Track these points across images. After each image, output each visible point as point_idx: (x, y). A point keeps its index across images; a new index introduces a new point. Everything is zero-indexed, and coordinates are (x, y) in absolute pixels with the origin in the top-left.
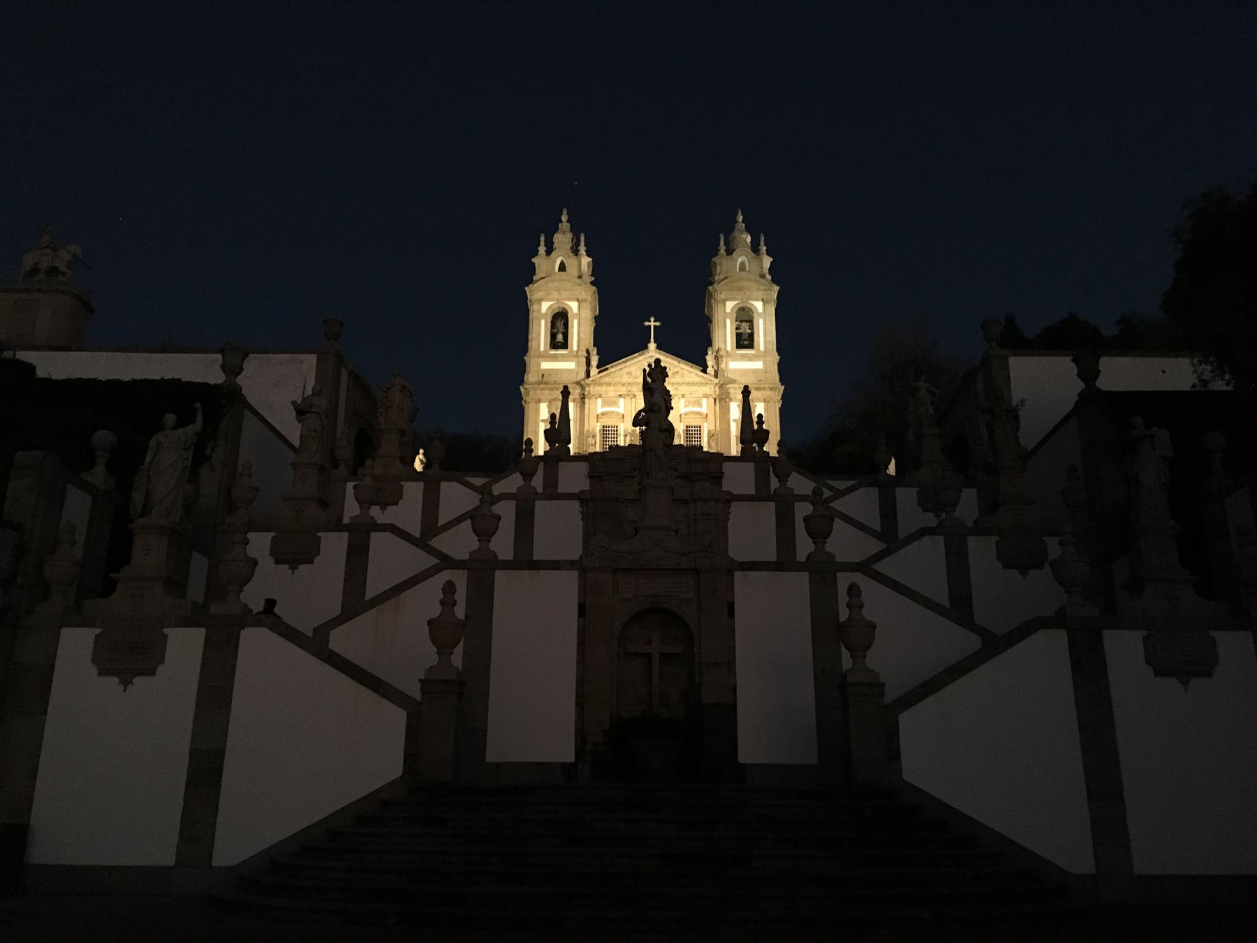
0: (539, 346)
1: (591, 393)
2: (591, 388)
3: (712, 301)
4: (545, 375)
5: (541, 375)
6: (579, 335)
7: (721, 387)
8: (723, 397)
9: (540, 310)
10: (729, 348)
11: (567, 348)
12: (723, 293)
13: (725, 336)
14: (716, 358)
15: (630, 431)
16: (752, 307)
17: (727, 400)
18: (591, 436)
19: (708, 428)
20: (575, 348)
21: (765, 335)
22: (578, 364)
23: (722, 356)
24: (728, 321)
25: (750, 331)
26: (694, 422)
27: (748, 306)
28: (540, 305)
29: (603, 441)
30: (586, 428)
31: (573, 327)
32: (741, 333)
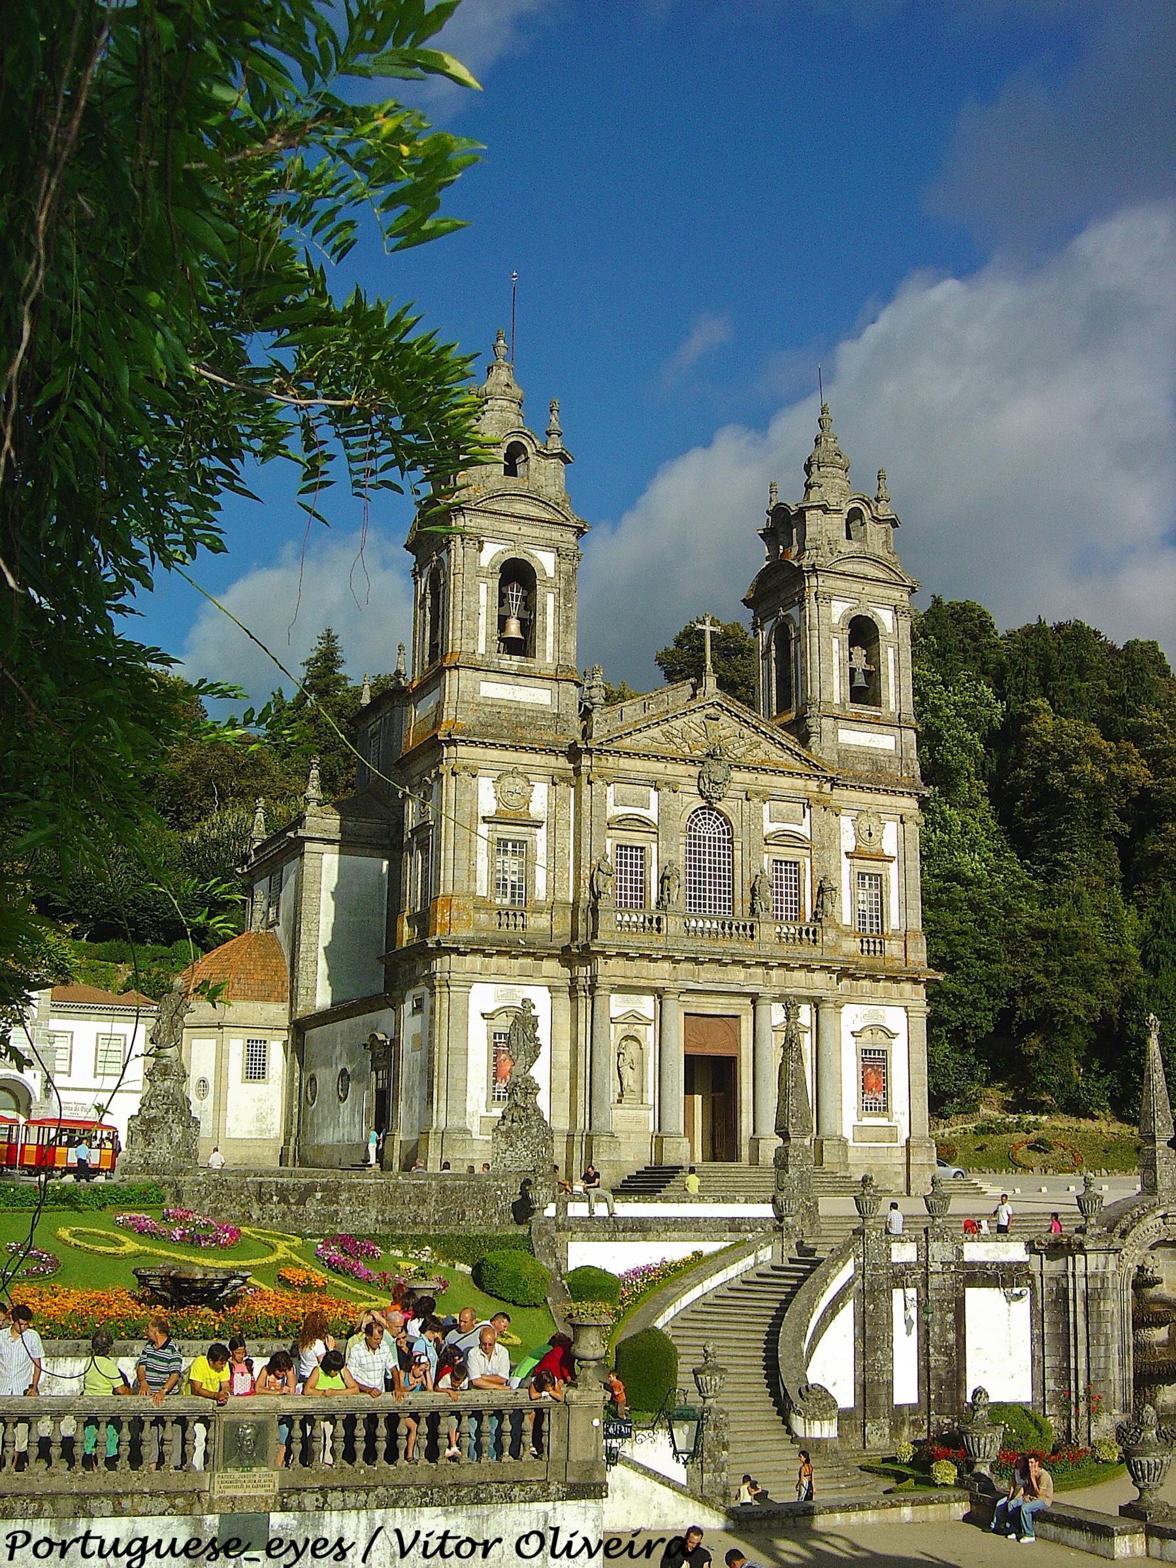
9: (476, 560)
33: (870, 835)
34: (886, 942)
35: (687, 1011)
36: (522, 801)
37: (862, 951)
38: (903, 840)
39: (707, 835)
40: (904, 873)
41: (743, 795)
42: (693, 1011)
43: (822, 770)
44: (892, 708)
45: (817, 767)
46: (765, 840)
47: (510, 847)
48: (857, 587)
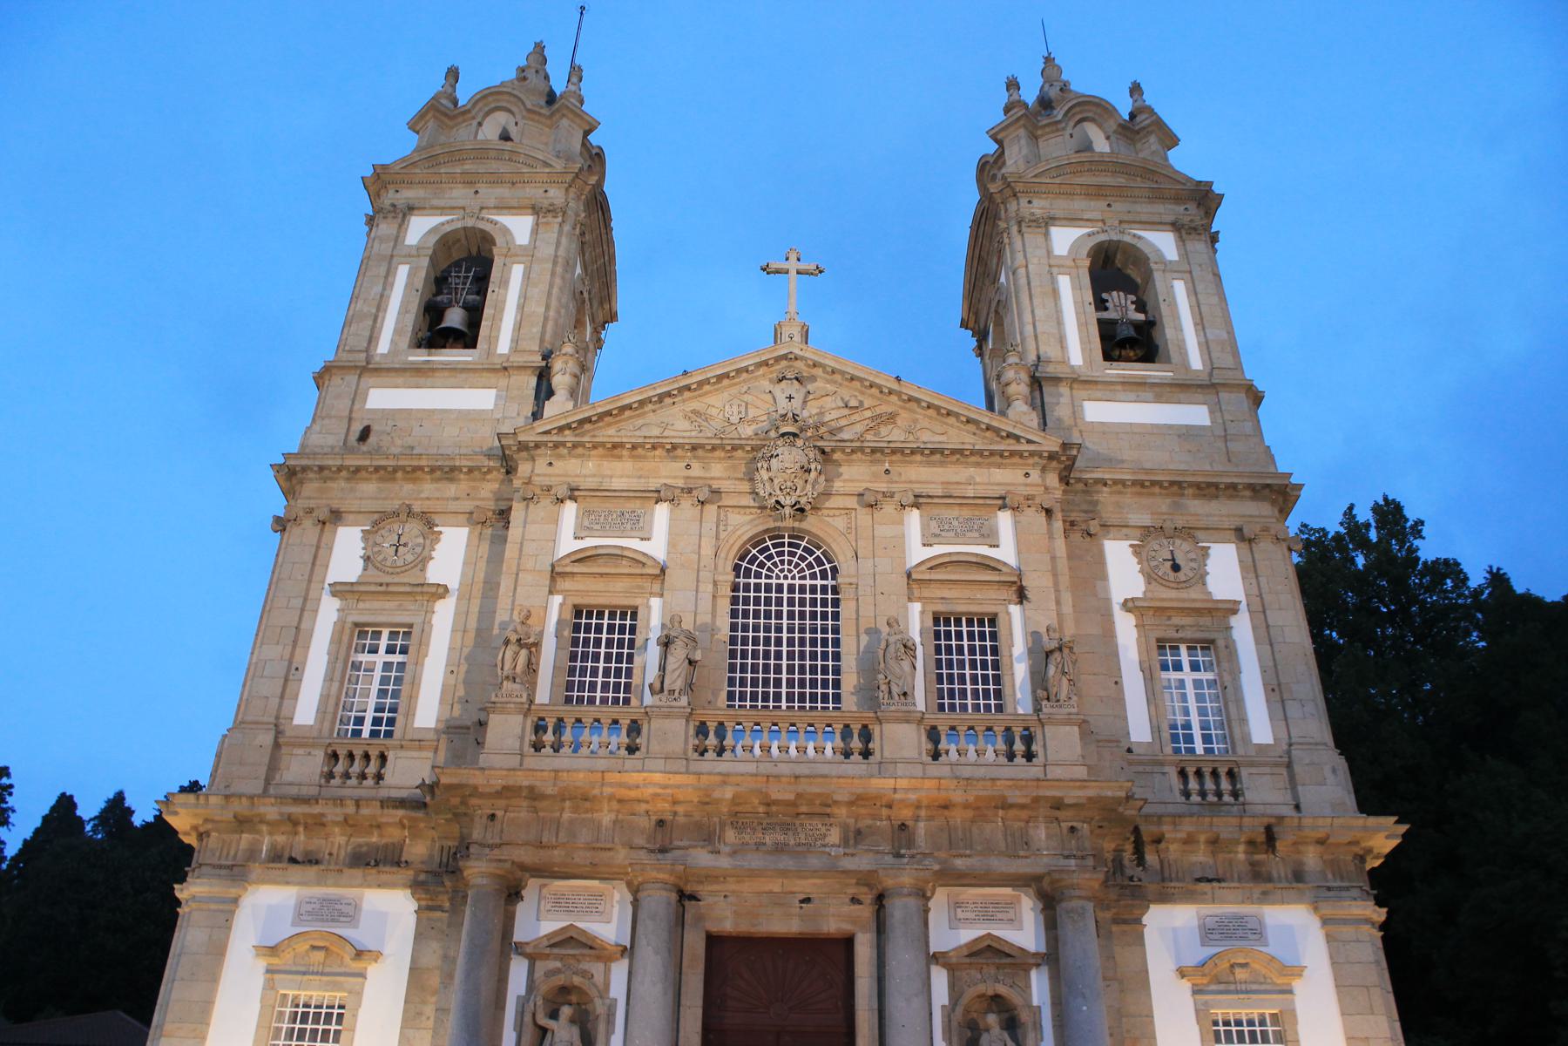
0: (372, 339)
1: (536, 479)
2: (541, 466)
3: (1002, 225)
4: (375, 428)
5: (357, 428)
6: (521, 308)
7: (1065, 480)
8: (1073, 516)
9: (398, 239)
10: (1076, 357)
11: (474, 346)
12: (1036, 202)
13: (1059, 323)
14: (1036, 383)
15: (688, 625)
16: (1139, 245)
17: (1094, 526)
18: (514, 638)
19: (1026, 621)
20: (504, 346)
21: (1200, 323)
22: (504, 398)
23: (1056, 380)
24: (1064, 283)
25: (1141, 317)
26: (962, 601)
27: (1127, 239)
28: (402, 225)
29: (572, 671)
30: (502, 616)
31: (505, 283)
32: (1113, 322)
33: (1176, 568)
34: (1244, 773)
35: (714, 928)
36: (410, 558)
37: (1187, 794)
38: (1250, 569)
39: (786, 583)
40: (1266, 635)
41: (852, 502)
42: (728, 924)
43: (1029, 442)
44: (1196, 362)
45: (1017, 438)
46: (909, 575)
47: (384, 642)
48: (1095, 208)
